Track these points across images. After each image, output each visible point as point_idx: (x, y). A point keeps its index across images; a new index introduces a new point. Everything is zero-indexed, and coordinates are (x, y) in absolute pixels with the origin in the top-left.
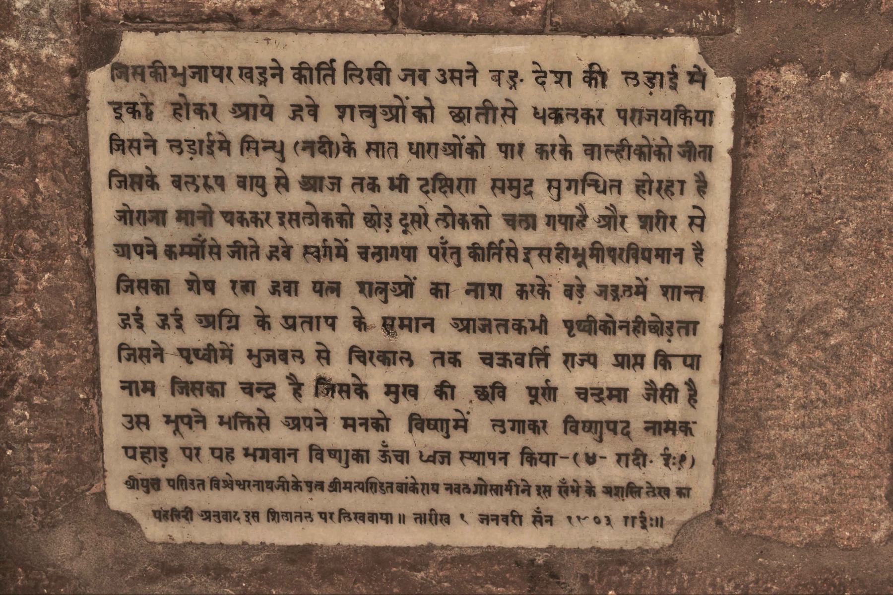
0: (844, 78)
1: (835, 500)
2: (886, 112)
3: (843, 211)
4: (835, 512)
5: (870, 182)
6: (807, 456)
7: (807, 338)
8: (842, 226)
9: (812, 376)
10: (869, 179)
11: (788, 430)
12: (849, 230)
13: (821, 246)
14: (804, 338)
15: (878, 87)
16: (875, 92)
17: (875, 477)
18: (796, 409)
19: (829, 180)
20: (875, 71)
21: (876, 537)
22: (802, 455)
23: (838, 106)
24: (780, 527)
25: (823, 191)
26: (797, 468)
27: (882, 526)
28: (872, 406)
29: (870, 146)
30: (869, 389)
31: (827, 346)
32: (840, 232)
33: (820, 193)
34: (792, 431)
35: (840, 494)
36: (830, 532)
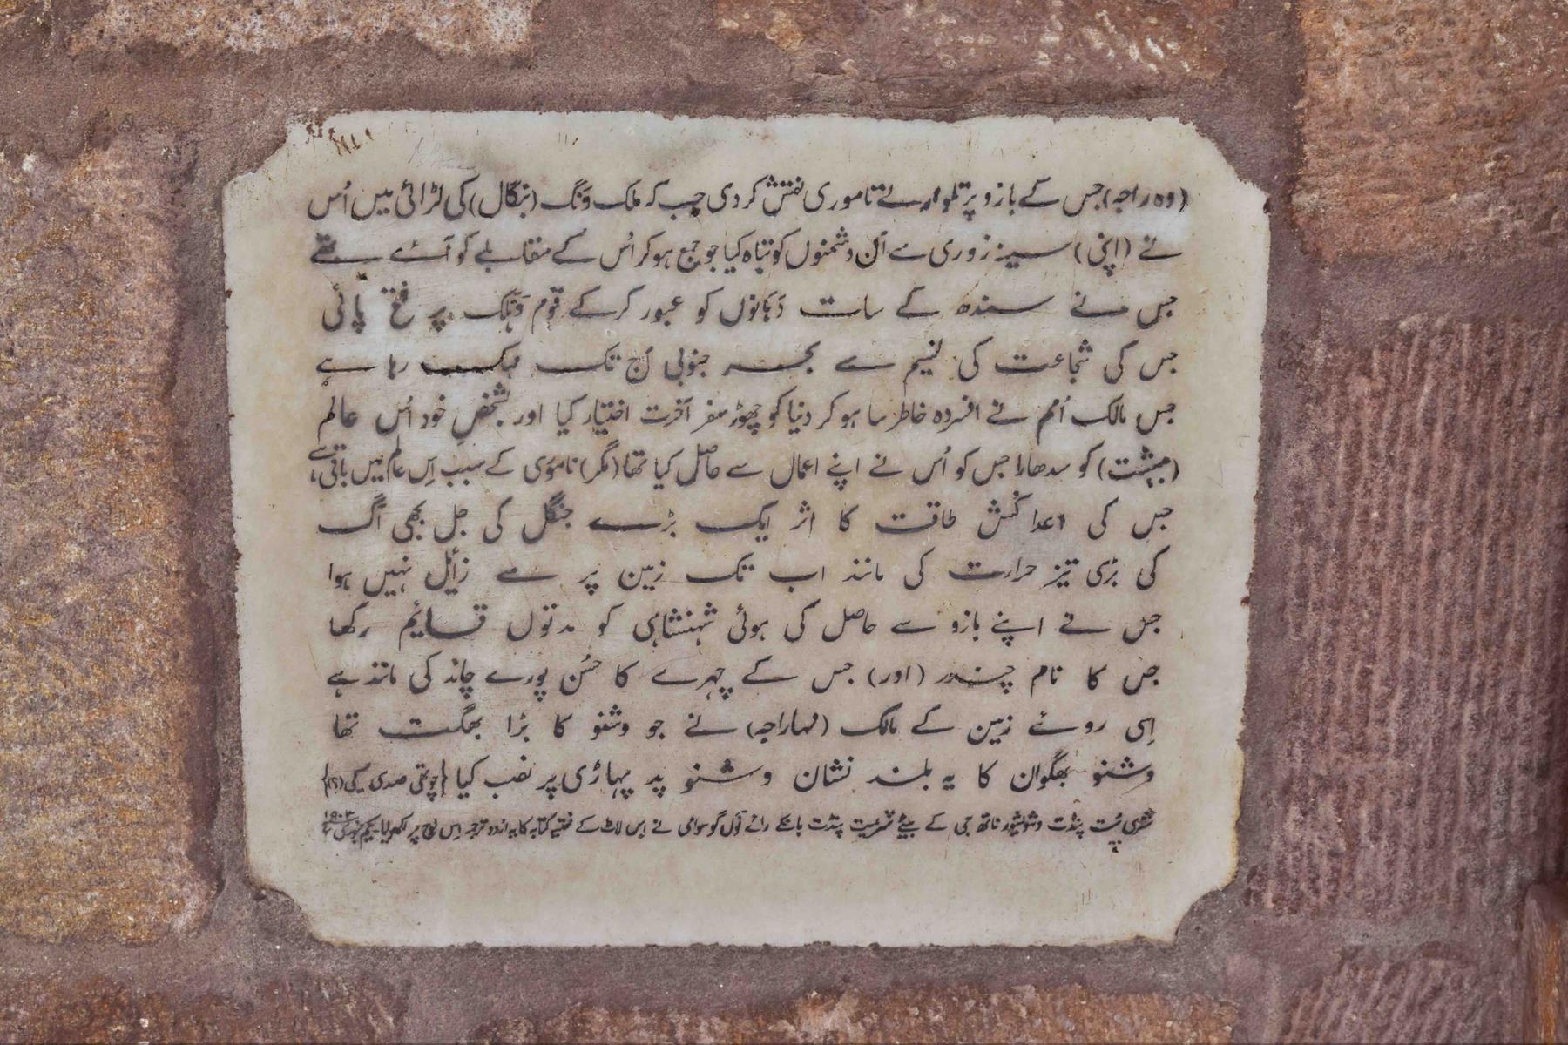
0: (29, 163)
1: (104, 863)
2: (106, 217)
3: (55, 384)
4: (106, 883)
5: (93, 333)
6: (44, 790)
7: (24, 594)
8: (56, 408)
9: (41, 658)
10: (89, 329)
11: (9, 748)
12: (70, 413)
13: (26, 442)
14: (18, 594)
15: (88, 177)
16: (84, 187)
17: (165, 823)
18: (20, 714)
19: (24, 331)
20: (78, 151)
21: (180, 923)
22: (39, 790)
23: (25, 209)
24: (18, 910)
25: (17, 350)
26: (34, 812)
27: (189, 905)
28: (145, 704)
29: (86, 274)
30: (135, 677)
31: (60, 606)
32: (54, 416)
33: (11, 352)
34: (18, 750)
35: (111, 853)
36: (100, 916)
